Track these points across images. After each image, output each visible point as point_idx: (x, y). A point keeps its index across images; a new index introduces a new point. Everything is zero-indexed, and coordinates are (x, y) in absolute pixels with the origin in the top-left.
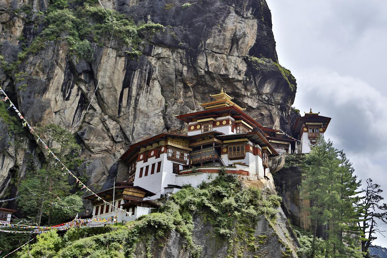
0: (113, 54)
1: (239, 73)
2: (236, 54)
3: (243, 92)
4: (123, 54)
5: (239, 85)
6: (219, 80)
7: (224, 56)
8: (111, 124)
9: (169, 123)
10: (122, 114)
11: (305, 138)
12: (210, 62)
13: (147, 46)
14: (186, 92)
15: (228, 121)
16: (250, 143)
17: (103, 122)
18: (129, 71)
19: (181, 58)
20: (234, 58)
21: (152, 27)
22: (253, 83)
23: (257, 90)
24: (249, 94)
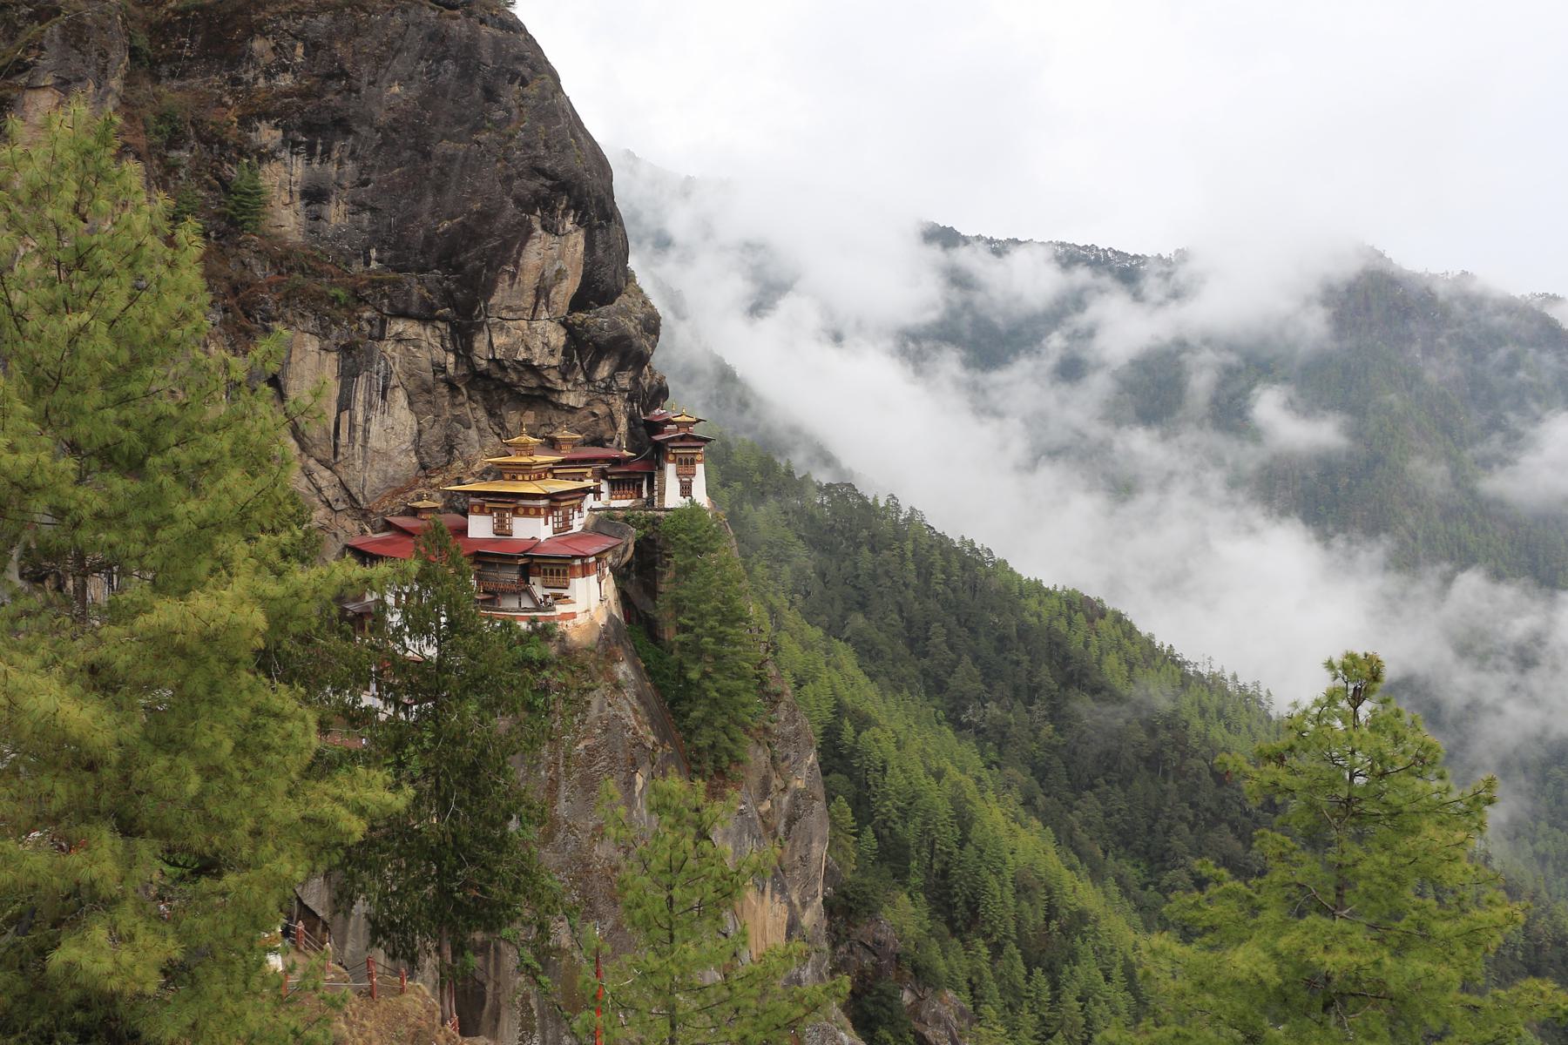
0: (313, 344)
1: (552, 353)
2: (545, 315)
3: (560, 385)
4: (333, 347)
5: (553, 375)
6: (515, 369)
7: (523, 323)
8: (324, 477)
9: (427, 459)
10: (340, 458)
11: (670, 469)
12: (497, 341)
13: (377, 323)
14: (453, 397)
15: (538, 510)
16: (578, 562)
17: (309, 474)
18: (348, 376)
19: (442, 338)
20: (541, 324)
21: (382, 283)
22: (578, 368)
23: (586, 375)
24: (570, 386)
